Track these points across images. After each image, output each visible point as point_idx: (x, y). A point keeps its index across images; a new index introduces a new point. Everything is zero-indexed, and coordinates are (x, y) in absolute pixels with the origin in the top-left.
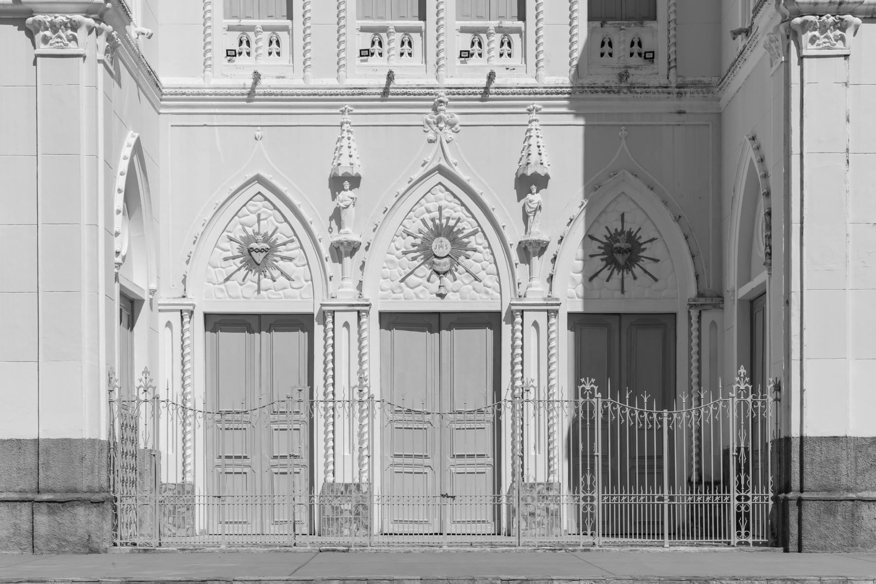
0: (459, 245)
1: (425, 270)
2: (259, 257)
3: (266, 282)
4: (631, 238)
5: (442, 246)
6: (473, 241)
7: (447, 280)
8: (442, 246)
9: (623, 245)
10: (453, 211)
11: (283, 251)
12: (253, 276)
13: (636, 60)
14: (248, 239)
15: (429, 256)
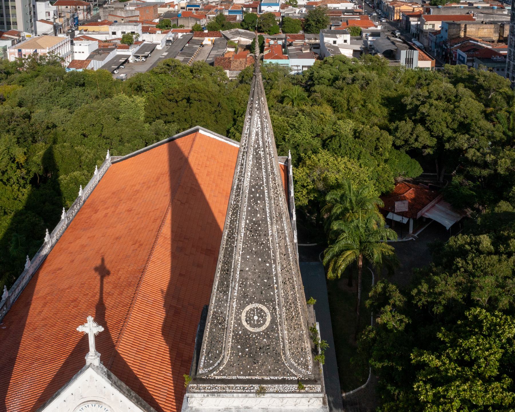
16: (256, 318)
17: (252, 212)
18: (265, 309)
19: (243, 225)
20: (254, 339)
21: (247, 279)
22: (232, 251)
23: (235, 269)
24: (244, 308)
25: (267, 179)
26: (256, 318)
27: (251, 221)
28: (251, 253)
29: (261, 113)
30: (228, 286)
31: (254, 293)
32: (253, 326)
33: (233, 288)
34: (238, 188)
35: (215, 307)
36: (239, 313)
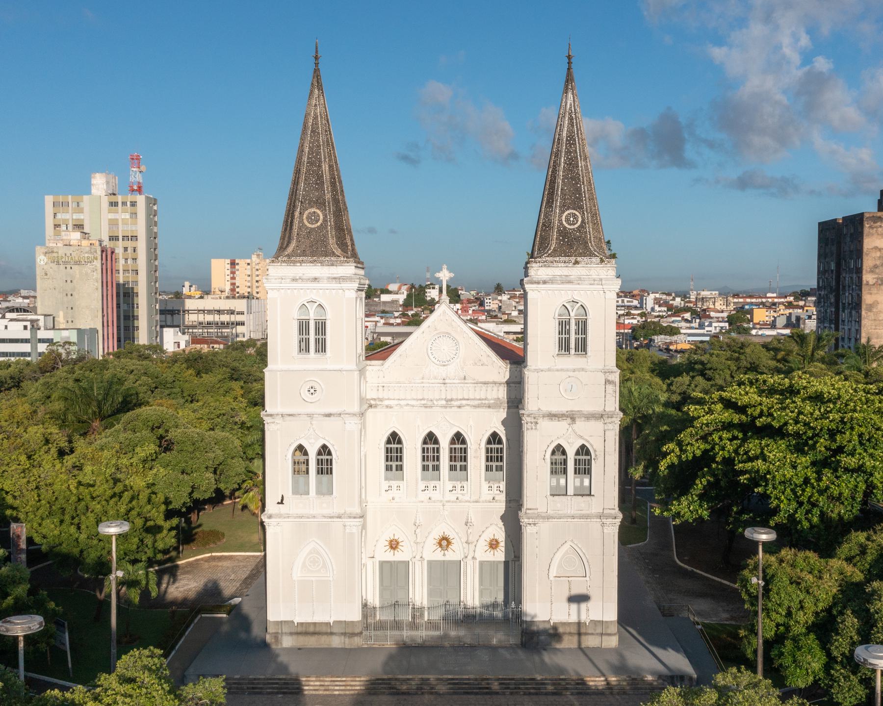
0: (449, 543)
1: (440, 549)
2: (394, 546)
3: (396, 552)
4: (496, 541)
5: (444, 543)
6: (453, 541)
7: (446, 552)
8: (444, 543)
9: (494, 543)
10: (447, 534)
11: (401, 544)
12: (392, 551)
13: (498, 492)
14: (391, 541)
15: (440, 545)
16: (572, 219)
17: (568, 152)
18: (577, 213)
19: (563, 160)
20: (570, 233)
21: (565, 195)
22: (555, 179)
23: (558, 188)
24: (564, 212)
25: (577, 132)
26: (572, 219)
27: (567, 158)
28: (567, 178)
29: (573, 91)
30: (553, 201)
31: (570, 203)
32: (570, 225)
33: (557, 201)
34: (559, 139)
35: (544, 219)
36: (560, 216)
